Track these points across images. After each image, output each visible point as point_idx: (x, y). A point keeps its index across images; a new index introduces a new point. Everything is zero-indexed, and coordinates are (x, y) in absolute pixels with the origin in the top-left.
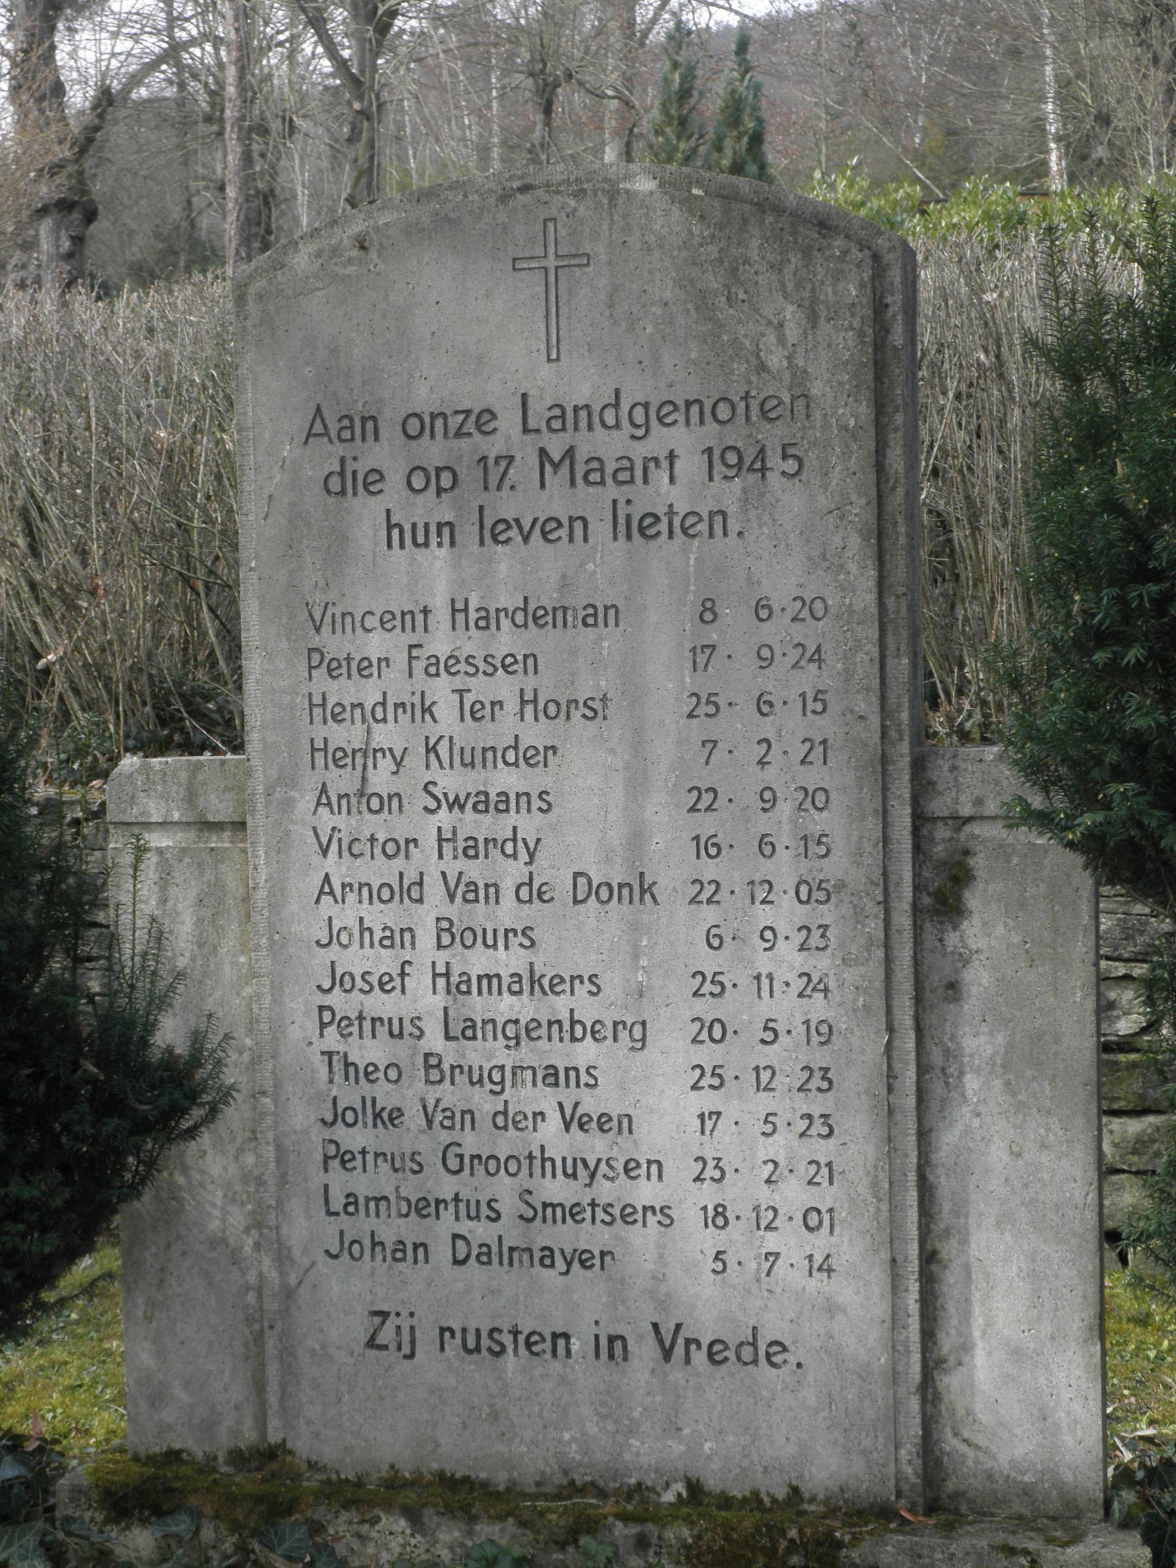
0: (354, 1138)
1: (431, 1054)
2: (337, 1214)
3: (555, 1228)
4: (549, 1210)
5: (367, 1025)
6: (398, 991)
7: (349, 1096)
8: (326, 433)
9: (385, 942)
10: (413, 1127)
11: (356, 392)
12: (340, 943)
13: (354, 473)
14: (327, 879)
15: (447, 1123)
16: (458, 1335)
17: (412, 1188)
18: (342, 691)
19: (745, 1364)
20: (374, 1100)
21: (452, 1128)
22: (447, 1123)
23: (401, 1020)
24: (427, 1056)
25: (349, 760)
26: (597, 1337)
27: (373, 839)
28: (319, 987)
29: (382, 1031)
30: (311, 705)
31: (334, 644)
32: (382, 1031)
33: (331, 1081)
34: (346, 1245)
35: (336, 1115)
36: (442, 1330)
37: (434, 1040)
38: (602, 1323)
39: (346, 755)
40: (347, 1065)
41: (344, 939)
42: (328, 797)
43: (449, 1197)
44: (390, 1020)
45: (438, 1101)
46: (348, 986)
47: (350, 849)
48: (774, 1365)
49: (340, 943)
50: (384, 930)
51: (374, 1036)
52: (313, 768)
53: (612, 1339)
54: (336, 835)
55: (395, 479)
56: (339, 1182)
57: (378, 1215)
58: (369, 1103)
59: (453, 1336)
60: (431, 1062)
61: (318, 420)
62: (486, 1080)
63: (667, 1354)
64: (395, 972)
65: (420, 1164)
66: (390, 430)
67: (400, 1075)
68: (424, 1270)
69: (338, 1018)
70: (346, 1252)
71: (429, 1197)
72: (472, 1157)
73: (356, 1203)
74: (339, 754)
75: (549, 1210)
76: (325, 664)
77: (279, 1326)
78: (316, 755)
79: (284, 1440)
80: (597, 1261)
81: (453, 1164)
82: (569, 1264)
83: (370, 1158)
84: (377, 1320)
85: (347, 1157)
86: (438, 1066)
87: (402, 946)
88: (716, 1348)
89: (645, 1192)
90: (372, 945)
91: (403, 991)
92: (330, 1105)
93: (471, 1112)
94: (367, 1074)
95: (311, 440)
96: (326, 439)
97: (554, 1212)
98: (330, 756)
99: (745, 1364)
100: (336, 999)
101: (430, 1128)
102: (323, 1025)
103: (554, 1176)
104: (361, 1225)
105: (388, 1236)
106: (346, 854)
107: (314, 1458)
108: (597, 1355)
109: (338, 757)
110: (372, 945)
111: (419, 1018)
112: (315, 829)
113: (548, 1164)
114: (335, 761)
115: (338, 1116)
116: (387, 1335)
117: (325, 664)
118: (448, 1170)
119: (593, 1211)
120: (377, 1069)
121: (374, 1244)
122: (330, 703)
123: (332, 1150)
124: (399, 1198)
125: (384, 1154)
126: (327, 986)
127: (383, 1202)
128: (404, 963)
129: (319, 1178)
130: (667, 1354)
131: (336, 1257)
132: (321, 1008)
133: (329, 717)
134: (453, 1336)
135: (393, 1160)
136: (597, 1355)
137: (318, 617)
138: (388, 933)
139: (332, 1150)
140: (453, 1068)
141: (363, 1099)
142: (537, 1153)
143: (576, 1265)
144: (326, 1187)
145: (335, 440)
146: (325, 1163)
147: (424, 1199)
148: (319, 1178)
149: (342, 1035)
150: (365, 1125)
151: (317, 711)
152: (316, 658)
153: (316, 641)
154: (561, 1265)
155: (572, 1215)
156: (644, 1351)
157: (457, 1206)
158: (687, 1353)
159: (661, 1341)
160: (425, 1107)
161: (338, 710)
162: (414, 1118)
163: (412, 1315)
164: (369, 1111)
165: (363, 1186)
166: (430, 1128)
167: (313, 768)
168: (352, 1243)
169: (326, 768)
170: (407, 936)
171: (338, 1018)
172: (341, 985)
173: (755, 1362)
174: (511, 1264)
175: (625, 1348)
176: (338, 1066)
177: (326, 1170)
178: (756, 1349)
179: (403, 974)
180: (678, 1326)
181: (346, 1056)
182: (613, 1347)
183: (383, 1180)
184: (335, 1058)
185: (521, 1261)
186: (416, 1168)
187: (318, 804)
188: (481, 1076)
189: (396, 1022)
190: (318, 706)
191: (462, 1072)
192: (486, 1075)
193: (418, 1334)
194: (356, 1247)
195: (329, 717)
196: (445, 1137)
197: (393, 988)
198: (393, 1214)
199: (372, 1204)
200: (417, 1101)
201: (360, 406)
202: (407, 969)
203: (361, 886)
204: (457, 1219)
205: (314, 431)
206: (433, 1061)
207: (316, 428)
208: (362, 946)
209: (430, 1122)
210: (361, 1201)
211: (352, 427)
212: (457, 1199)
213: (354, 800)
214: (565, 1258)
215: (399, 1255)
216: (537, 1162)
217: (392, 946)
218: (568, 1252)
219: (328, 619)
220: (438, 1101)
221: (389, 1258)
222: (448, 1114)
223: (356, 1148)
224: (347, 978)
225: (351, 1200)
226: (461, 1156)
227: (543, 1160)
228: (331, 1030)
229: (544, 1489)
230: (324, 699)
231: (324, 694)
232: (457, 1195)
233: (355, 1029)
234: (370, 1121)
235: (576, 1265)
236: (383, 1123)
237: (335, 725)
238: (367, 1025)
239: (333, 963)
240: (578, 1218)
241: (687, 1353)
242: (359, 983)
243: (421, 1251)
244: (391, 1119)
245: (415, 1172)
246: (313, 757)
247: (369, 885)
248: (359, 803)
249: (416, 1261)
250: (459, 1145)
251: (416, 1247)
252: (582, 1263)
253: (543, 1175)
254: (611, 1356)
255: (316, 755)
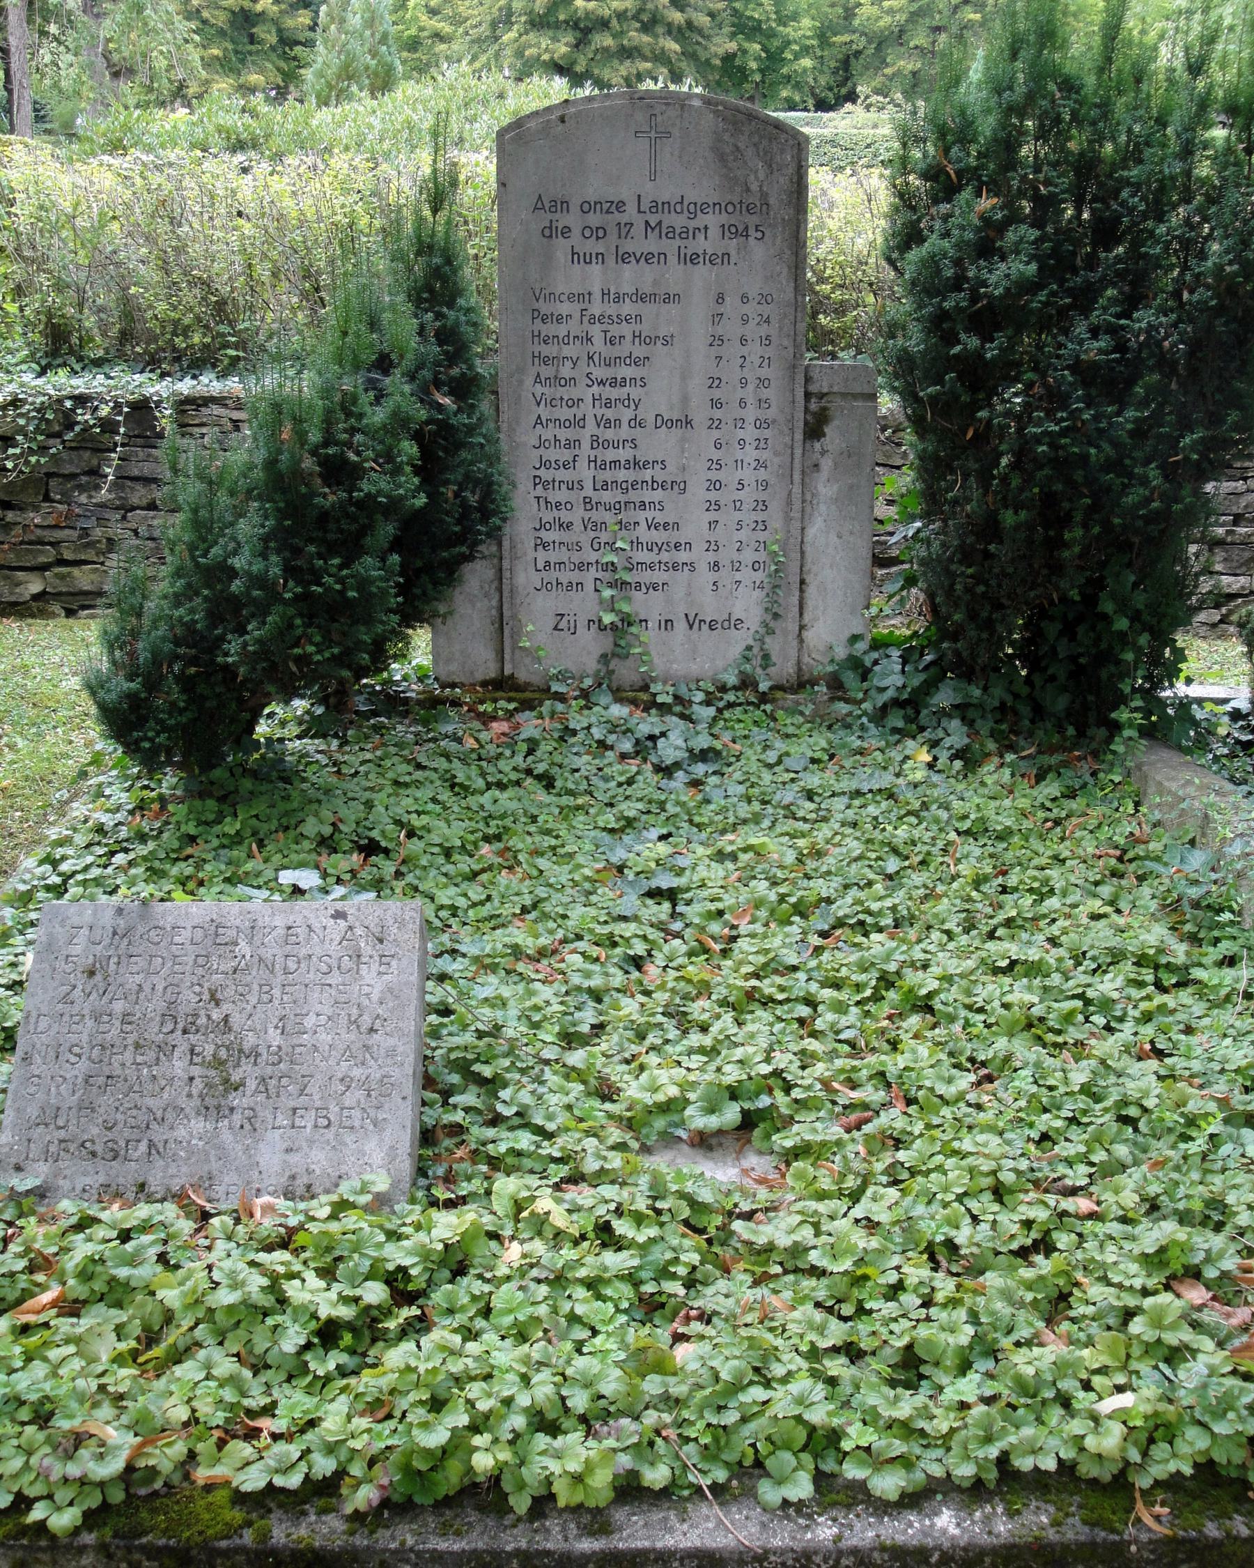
7: (548, 516)
17: (576, 558)
18: (549, 329)
31: (545, 308)
37: (588, 491)
55: (576, 232)
56: (542, 556)
60: (587, 501)
66: (575, 208)
89: (683, 556)
100: (542, 472)
104: (552, 575)
109: (546, 361)
115: (542, 526)
148: (531, 554)
156: (681, 625)
162: (577, 526)
165: (553, 556)
182: (668, 623)
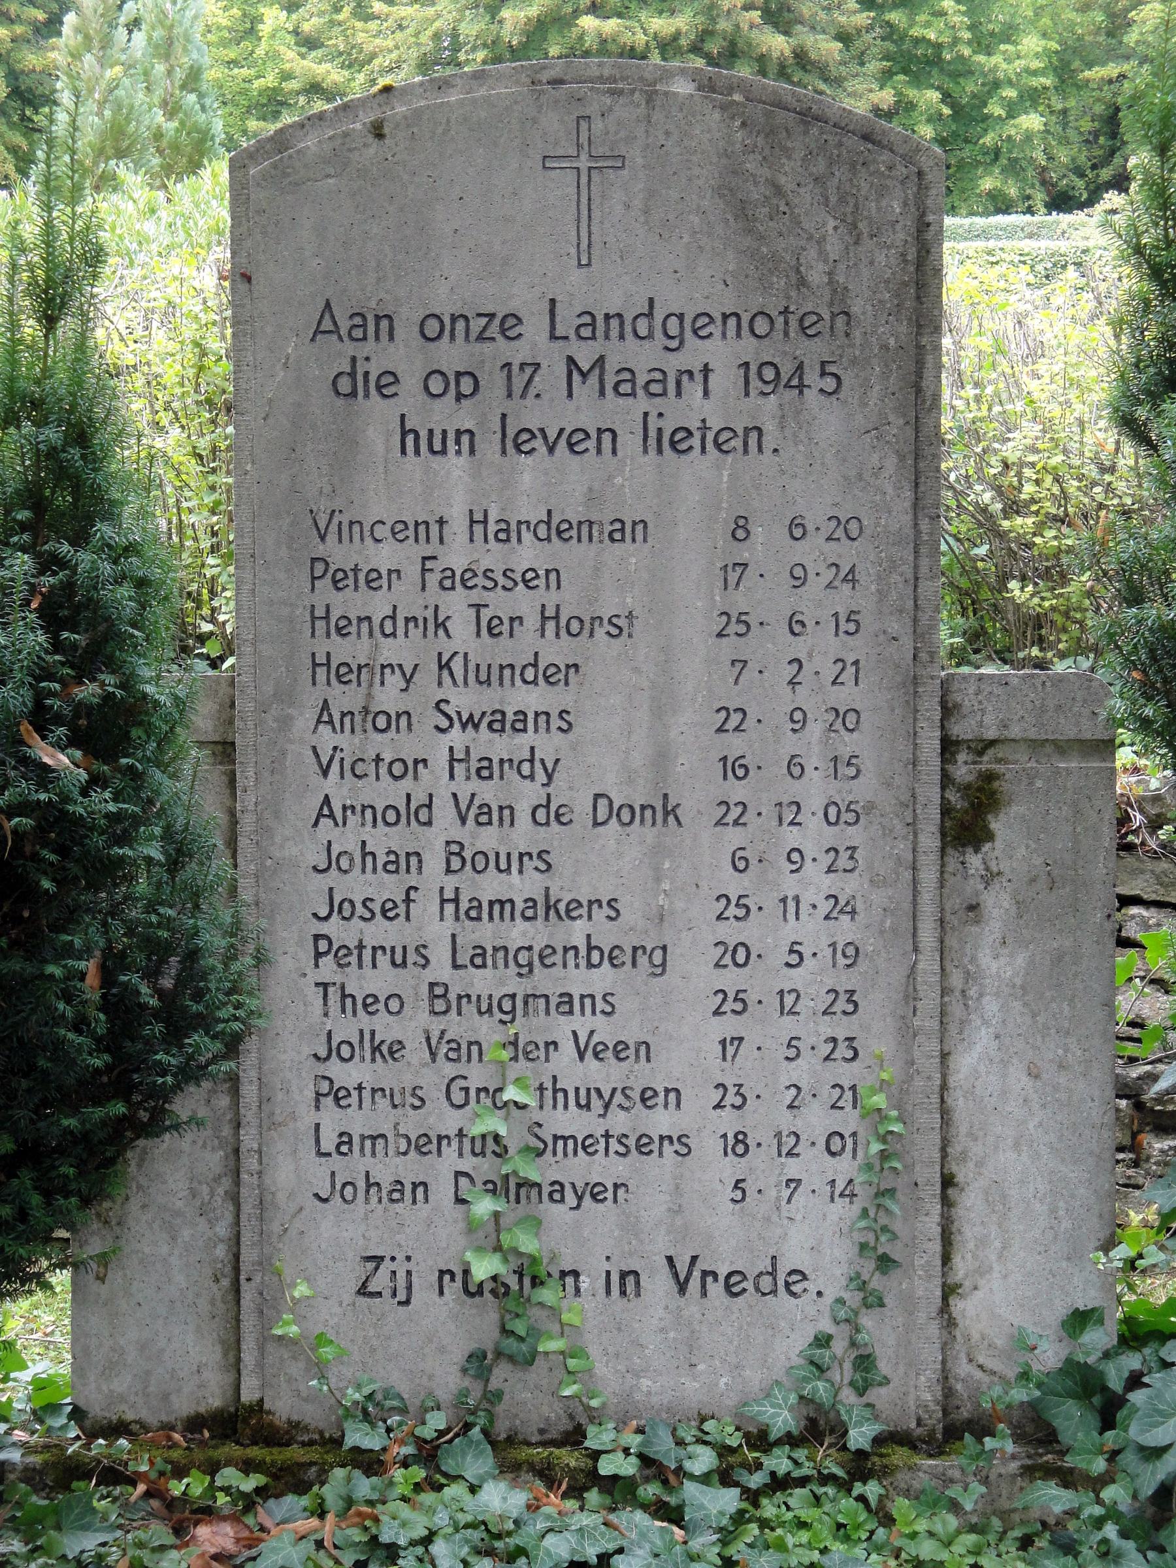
0: (346, 1074)
1: (437, 984)
2: (329, 1155)
3: (566, 1162)
4: (560, 1143)
5: (367, 954)
6: (402, 918)
7: (346, 1028)
8: (336, 330)
9: (389, 867)
10: (415, 1061)
11: (369, 288)
12: (340, 869)
13: (366, 374)
14: (327, 800)
15: (452, 1055)
16: (459, 1278)
17: (412, 1124)
18: (350, 602)
19: (764, 1294)
20: (373, 1033)
21: (458, 1060)
22: (452, 1055)
23: (404, 948)
24: (432, 985)
25: (353, 677)
26: (608, 1273)
27: (378, 759)
28: (315, 915)
29: (383, 960)
30: (314, 618)
31: (341, 555)
32: (383, 960)
33: (326, 1015)
34: (338, 1187)
35: (330, 1050)
36: (442, 1273)
37: (440, 968)
38: (613, 1259)
39: (351, 671)
40: (344, 996)
41: (344, 864)
42: (330, 715)
43: (452, 1132)
44: (393, 949)
45: (443, 1032)
46: (346, 914)
47: (353, 769)
48: (793, 1294)
49: (340, 869)
50: (388, 854)
51: (374, 966)
52: (314, 684)
53: (623, 1275)
54: (338, 755)
55: (411, 383)
56: (332, 1121)
57: (374, 1154)
58: (367, 1037)
59: (453, 1279)
60: (437, 992)
61: (327, 316)
62: (495, 1009)
63: (682, 1288)
64: (399, 898)
65: (422, 1099)
66: (406, 331)
67: (402, 1006)
68: (423, 1210)
69: (335, 947)
70: (338, 1195)
71: (431, 1134)
72: (479, 1090)
73: (350, 1142)
74: (343, 670)
75: (560, 1143)
76: (329, 575)
77: (257, 1279)
78: (318, 670)
79: (262, 1400)
80: (609, 1195)
81: (458, 1097)
82: (580, 1198)
83: (366, 1094)
84: (371, 1266)
85: (342, 1094)
86: (444, 996)
87: (408, 871)
88: (733, 1280)
89: (661, 1121)
90: (375, 870)
91: (408, 918)
92: (324, 1038)
93: (478, 1043)
94: (365, 1006)
95: (319, 337)
96: (335, 337)
97: (565, 1145)
98: (333, 671)
99: (764, 1294)
100: (333, 927)
101: (434, 1061)
102: (318, 955)
103: (566, 1107)
104: (356, 1165)
105: (384, 1174)
106: (348, 773)
107: (295, 1418)
108: (608, 1292)
109: (343, 674)
110: (375, 870)
111: (425, 947)
112: (314, 748)
113: (560, 1095)
114: (338, 676)
115: (333, 1051)
116: (380, 1282)
117: (329, 575)
118: (452, 1105)
119: (607, 1143)
120: (376, 1000)
121: (369, 1186)
122: (335, 615)
123: (325, 1087)
124: (398, 1135)
125: (383, 1090)
126: (323, 913)
127: (380, 1141)
128: (411, 888)
129: (308, 1117)
130: (682, 1288)
131: (326, 1200)
132: (317, 937)
133: (333, 631)
134: (453, 1279)
135: (392, 1096)
136: (608, 1292)
137: (322, 526)
138: (392, 858)
139: (325, 1087)
140: (460, 997)
141: (361, 1032)
142: (549, 1084)
143: (587, 1198)
144: (318, 1126)
145: (345, 339)
146: (317, 1101)
147: (425, 1135)
148: (308, 1117)
149: (340, 965)
150: (363, 1059)
151: (320, 624)
152: (319, 568)
153: (320, 550)
154: (571, 1199)
155: (584, 1148)
156: (658, 1284)
157: (461, 1142)
158: (704, 1286)
159: (676, 1275)
160: (428, 1039)
161: (342, 623)
162: (416, 1052)
163: (408, 1258)
164: (367, 1045)
165: (358, 1122)
166: (434, 1061)
167: (314, 684)
168: (344, 1185)
169: (329, 683)
170: (414, 860)
171: (335, 947)
172: (340, 911)
173: (774, 1292)
174: (518, 1201)
175: (638, 1283)
176: (334, 994)
177: (317, 1108)
178: (775, 1279)
179: (408, 900)
180: (694, 1259)
181: (343, 987)
182: (627, 1281)
183: (380, 1117)
184: (331, 990)
185: (528, 1198)
186: (417, 1103)
187: (319, 721)
188: (490, 1005)
189: (399, 951)
190: (319, 618)
191: (469, 1001)
192: (495, 1004)
193: (414, 1279)
194: (349, 1189)
195: (333, 631)
196: (450, 1070)
197: (397, 915)
198: (390, 1153)
199: (368, 1143)
200: (420, 1032)
201: (373, 304)
202: (413, 895)
203: (364, 808)
204: (461, 1155)
205: (322, 328)
206: (439, 991)
207: (325, 326)
208: (364, 871)
209: (433, 1055)
210: (356, 1140)
211: (364, 326)
212: (461, 1134)
213: (358, 718)
214: (576, 1192)
215: (396, 1196)
216: (549, 1094)
217: (397, 871)
218: (580, 1186)
219: (334, 527)
220: (443, 1032)
221: (385, 1200)
222: (454, 1045)
223: (351, 1084)
224: (346, 905)
225: (345, 1139)
226: (467, 1090)
227: (555, 1091)
228: (327, 961)
229: (548, 1436)
230: (328, 611)
231: (328, 606)
232: (461, 1130)
233: (353, 959)
234: (368, 1056)
235: (587, 1198)
236: (383, 1056)
237: (339, 639)
238: (367, 954)
239: (331, 889)
240: (590, 1150)
241: (704, 1286)
242: (360, 910)
243: (420, 1190)
244: (391, 1053)
245: (415, 1108)
246: (314, 673)
247: (372, 807)
248: (364, 721)
249: (414, 1202)
250: (465, 1078)
251: (415, 1186)
252: (594, 1196)
253: (555, 1107)
254: (623, 1293)
255: (318, 670)
